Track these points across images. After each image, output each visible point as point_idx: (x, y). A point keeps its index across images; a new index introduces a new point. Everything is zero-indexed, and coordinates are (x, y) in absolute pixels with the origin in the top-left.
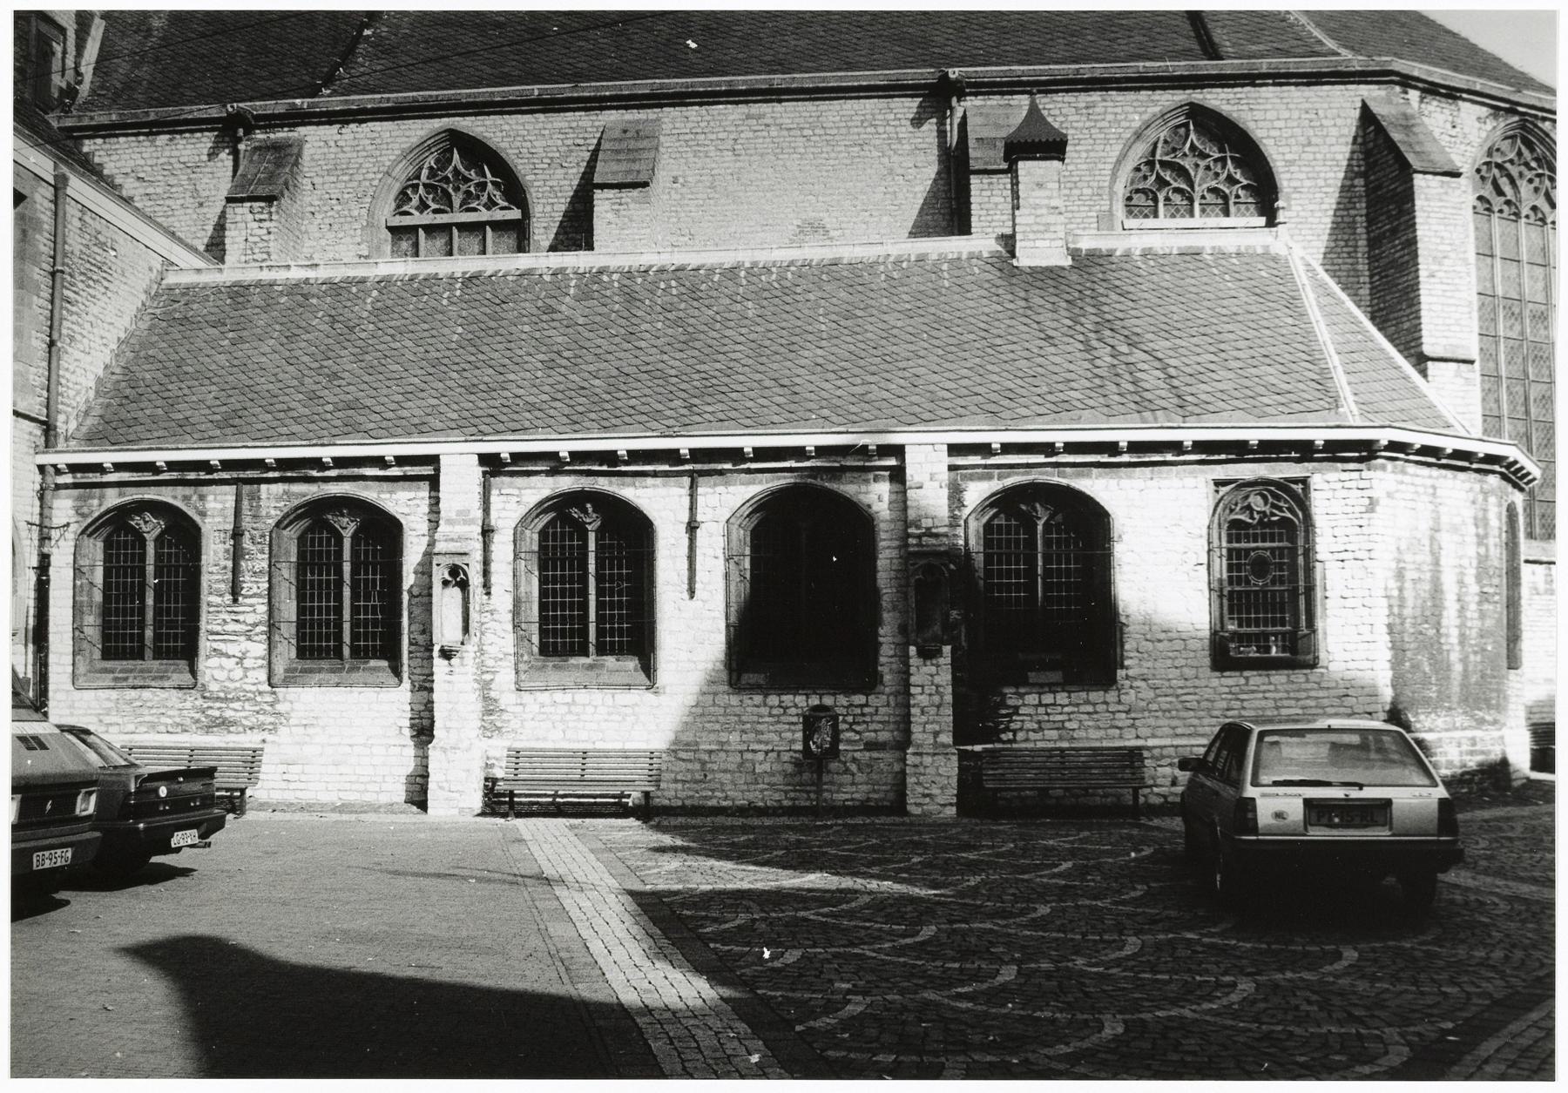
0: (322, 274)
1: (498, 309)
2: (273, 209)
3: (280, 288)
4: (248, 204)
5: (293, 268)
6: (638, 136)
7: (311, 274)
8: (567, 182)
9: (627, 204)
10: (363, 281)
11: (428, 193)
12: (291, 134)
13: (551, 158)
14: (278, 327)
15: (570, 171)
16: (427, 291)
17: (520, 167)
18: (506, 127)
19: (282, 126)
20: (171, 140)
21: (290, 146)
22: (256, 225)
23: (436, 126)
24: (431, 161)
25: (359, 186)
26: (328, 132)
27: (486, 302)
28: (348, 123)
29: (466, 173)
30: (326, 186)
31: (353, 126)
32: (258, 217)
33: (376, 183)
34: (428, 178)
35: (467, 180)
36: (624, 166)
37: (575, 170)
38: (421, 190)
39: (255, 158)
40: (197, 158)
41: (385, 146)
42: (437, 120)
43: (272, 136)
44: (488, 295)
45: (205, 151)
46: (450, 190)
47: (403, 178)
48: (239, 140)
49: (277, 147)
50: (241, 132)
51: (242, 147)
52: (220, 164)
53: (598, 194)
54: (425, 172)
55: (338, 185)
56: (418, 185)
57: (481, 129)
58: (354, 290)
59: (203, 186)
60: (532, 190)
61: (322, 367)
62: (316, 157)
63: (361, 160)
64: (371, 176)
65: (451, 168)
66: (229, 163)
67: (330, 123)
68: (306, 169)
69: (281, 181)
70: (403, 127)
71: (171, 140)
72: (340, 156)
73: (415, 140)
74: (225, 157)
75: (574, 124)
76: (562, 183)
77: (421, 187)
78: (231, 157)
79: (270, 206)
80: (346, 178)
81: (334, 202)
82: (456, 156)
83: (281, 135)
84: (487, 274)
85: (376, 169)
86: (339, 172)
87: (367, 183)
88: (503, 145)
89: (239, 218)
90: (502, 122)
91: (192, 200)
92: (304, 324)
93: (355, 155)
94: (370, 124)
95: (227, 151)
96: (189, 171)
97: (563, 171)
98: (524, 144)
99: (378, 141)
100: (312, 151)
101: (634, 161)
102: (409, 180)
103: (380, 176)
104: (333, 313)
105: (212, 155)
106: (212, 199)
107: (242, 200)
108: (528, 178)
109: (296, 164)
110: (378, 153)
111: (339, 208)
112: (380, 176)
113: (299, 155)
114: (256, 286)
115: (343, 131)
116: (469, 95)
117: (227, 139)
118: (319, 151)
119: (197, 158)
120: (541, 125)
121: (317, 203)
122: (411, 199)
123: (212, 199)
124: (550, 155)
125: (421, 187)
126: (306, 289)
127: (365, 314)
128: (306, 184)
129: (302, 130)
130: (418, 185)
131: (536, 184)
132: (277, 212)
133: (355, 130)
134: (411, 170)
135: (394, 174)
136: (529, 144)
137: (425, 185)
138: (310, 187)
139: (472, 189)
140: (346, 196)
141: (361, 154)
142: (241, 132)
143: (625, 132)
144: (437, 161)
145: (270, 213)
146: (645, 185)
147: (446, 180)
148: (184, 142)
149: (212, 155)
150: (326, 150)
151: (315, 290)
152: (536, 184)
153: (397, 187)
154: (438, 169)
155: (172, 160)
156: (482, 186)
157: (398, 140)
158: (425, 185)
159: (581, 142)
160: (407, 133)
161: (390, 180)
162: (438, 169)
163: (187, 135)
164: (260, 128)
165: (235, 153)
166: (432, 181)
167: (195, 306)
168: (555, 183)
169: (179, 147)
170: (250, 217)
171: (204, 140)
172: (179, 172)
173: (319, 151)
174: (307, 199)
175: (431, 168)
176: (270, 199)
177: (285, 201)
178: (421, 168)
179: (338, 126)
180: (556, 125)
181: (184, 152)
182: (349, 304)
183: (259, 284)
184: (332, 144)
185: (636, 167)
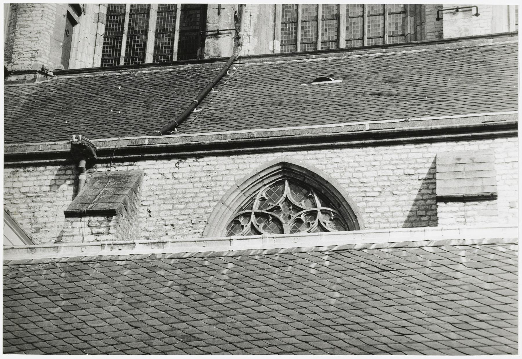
0: (170, 250)
1: (377, 276)
2: (111, 224)
3: (124, 263)
4: (87, 219)
5: (138, 245)
6: (473, 162)
7: (158, 251)
8: (399, 208)
9: (473, 216)
10: (217, 256)
11: (260, 222)
12: (130, 168)
13: (382, 187)
14: (120, 295)
15: (402, 198)
16: (291, 263)
17: (350, 195)
18: (338, 160)
19: (123, 161)
20: (14, 173)
21: (130, 176)
22: (93, 237)
23: (270, 159)
24: (263, 192)
25: (194, 213)
26: (166, 166)
27: (363, 271)
28: (185, 157)
29: (297, 204)
30: (162, 214)
31: (190, 160)
32: (95, 230)
33: (209, 210)
34: (259, 208)
35: (297, 209)
36: (466, 183)
37: (405, 198)
38: (253, 218)
39: (96, 184)
40: (38, 189)
41: (220, 178)
42: (270, 155)
43: (113, 169)
44: (363, 265)
45: (48, 183)
46: (281, 219)
47: (236, 207)
48: (80, 171)
49: (115, 177)
50: (83, 164)
51: (83, 177)
52: (60, 194)
53: (441, 206)
54: (257, 203)
55: (174, 212)
56: (250, 213)
57: (315, 162)
58: (206, 263)
59: (42, 214)
60: (364, 216)
61: (174, 329)
62: (154, 188)
63: (196, 190)
64: (206, 204)
65: (282, 199)
66: (70, 192)
67: (169, 158)
68: (142, 198)
69: (122, 199)
70: (238, 161)
71: (14, 173)
72: (177, 186)
73: (250, 173)
74: (67, 188)
75: (404, 156)
76: (393, 209)
77: (253, 216)
78: (72, 188)
79: (110, 221)
80: (181, 206)
81: (169, 227)
82: (287, 188)
83: (122, 168)
84: (356, 247)
85: (211, 198)
86: (175, 201)
87: (202, 211)
88: (335, 176)
89: (76, 232)
90: (333, 155)
91: (29, 226)
92: (151, 292)
93: (191, 185)
94: (206, 159)
95: (68, 182)
96: (29, 200)
97: (394, 198)
98: (355, 175)
99: (213, 173)
100: (150, 182)
101: (475, 179)
102: (241, 209)
103: (215, 204)
104: (184, 282)
105: (55, 185)
106: (48, 225)
107: (80, 215)
108: (359, 205)
109: (135, 190)
110: (213, 184)
111: (173, 233)
112: (215, 204)
113: (138, 183)
114: (95, 262)
115: (181, 165)
116: (302, 131)
117: (69, 172)
118: (157, 182)
119: (38, 189)
120: (371, 158)
121: (151, 229)
122: (243, 227)
123: (48, 225)
124: (381, 184)
125: (253, 216)
126: (152, 263)
127: (221, 283)
128: (143, 213)
129: (141, 165)
130: (250, 213)
131: (367, 210)
132: (115, 227)
133: (192, 164)
134: (243, 200)
135: (228, 203)
136: (360, 175)
137: (257, 215)
138: (146, 214)
139: (302, 217)
140: (181, 222)
141: (196, 185)
142: (83, 164)
143: (459, 159)
144: (269, 193)
145: (109, 227)
146: (492, 197)
147: (277, 209)
148: (27, 174)
149: (55, 185)
150: (163, 182)
151: (160, 264)
152: (367, 210)
153: (230, 216)
154: (270, 200)
155: (13, 191)
156: (313, 214)
157: (232, 172)
158: (257, 215)
159: (412, 172)
160: (241, 166)
161: (224, 208)
162: (270, 200)
163: (31, 169)
164: (101, 162)
165: (76, 184)
166: (264, 211)
167: (23, 280)
168: (386, 209)
169: (21, 179)
170: (88, 230)
171: (46, 173)
172: (19, 201)
173: (157, 182)
174: (143, 225)
175: (263, 199)
176: (109, 214)
177: (123, 219)
178: (253, 199)
179: (175, 161)
180: (386, 157)
181: (25, 184)
182: (202, 274)
183: (99, 260)
184: (170, 176)
185: (479, 183)
